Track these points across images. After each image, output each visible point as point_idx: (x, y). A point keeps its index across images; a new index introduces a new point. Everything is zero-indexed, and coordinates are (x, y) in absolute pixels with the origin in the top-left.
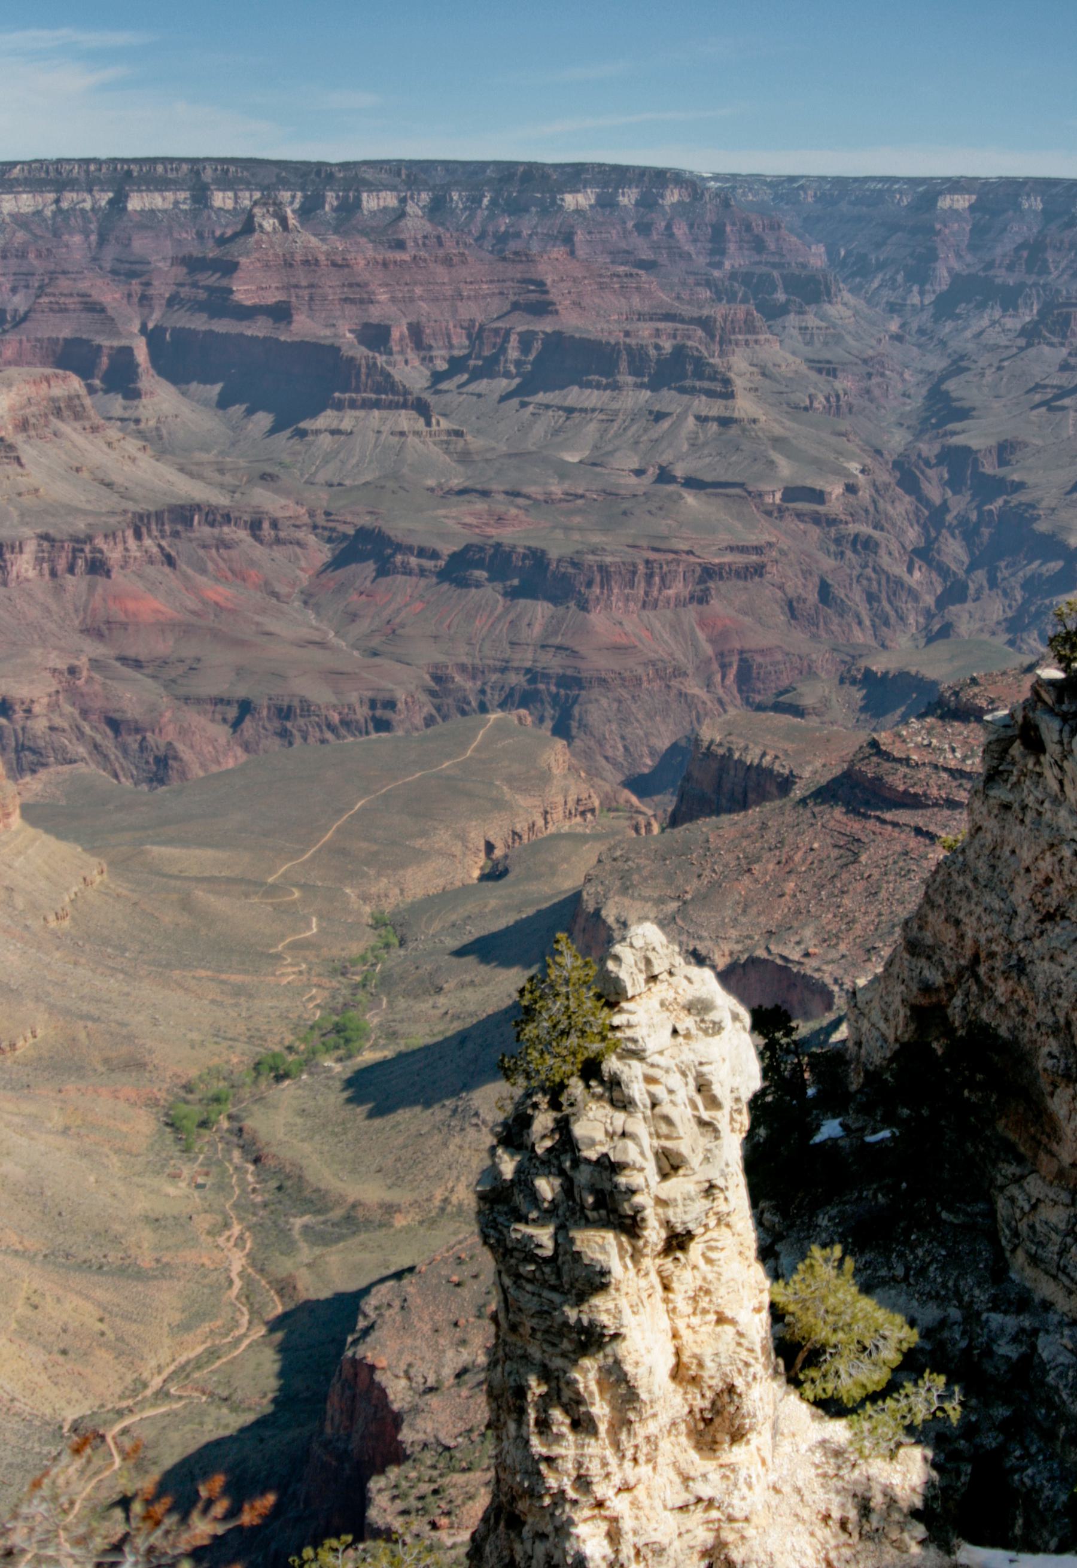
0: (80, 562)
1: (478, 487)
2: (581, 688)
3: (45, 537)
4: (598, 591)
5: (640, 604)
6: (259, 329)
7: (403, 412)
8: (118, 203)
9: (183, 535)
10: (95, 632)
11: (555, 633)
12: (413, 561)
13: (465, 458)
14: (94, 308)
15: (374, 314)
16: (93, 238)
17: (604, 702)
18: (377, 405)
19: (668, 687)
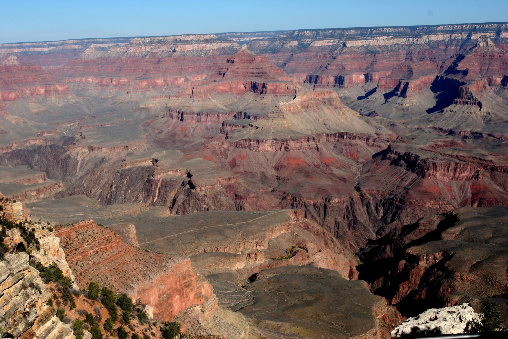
0: (283, 147)
1: (480, 132)
2: (404, 204)
3: (276, 140)
5: (451, 178)
8: (469, 37)
9: (340, 141)
10: (277, 169)
13: (488, 122)
14: (410, 70)
18: (467, 103)
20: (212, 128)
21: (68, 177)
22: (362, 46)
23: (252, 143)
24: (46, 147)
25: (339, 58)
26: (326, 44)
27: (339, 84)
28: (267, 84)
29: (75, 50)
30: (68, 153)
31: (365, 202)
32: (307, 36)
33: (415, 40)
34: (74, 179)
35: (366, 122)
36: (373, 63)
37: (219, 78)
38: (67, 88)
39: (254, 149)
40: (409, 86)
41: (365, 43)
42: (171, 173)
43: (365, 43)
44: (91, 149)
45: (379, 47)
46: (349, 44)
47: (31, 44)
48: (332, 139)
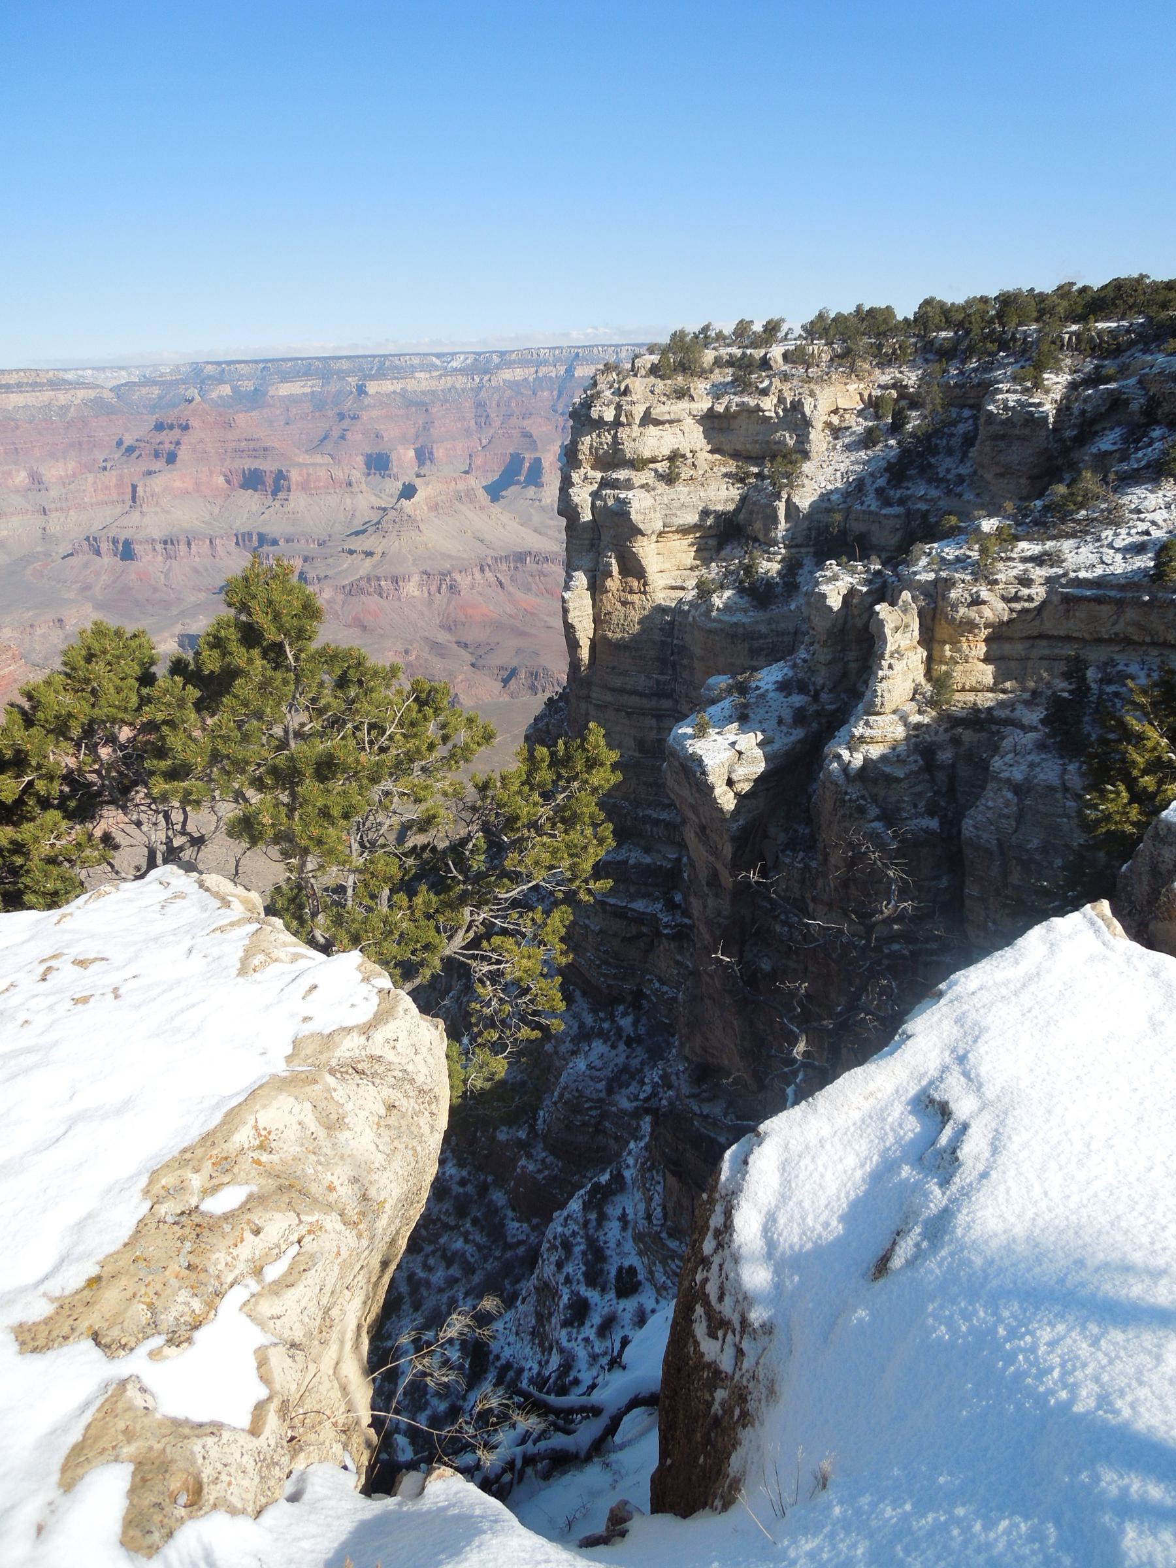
0: (444, 586)
3: (425, 573)
8: (570, 371)
14: (527, 435)
16: (555, 393)
20: (207, 570)
22: (394, 392)
23: (383, 583)
25: (365, 416)
26: (300, 391)
28: (288, 471)
32: (242, 376)
33: (486, 378)
35: (535, 531)
36: (427, 425)
37: (159, 464)
39: (388, 594)
41: (397, 386)
43: (397, 386)
45: (423, 393)
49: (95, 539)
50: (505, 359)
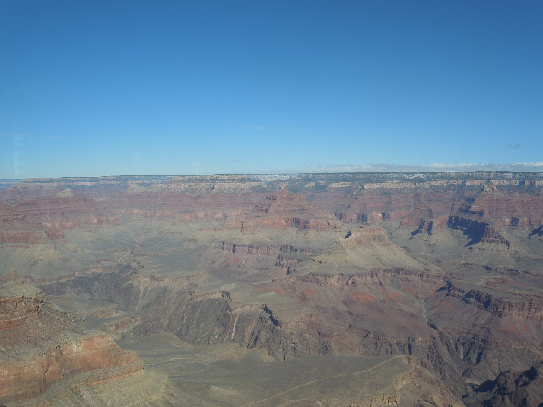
1: (516, 269)
2: (488, 344)
3: (342, 275)
4: (507, 311)
5: (526, 317)
6: (473, 218)
7: (501, 244)
10: (346, 303)
11: (488, 323)
12: (457, 293)
13: (518, 260)
14: (430, 210)
15: (515, 215)
17: (495, 351)
18: (494, 241)
19: (525, 349)
20: (263, 260)
21: (131, 306)
22: (377, 188)
23: (319, 277)
24: (106, 275)
27: (363, 220)
29: (114, 185)
30: (130, 282)
31: (444, 340)
33: (421, 184)
34: (137, 308)
35: (413, 257)
38: (116, 219)
40: (433, 225)
41: (379, 186)
42: (247, 308)
43: (379, 186)
44: (154, 278)
45: (391, 189)
46: (367, 186)
47: (75, 179)
48: (389, 274)
49: (223, 243)
50: (434, 176)
